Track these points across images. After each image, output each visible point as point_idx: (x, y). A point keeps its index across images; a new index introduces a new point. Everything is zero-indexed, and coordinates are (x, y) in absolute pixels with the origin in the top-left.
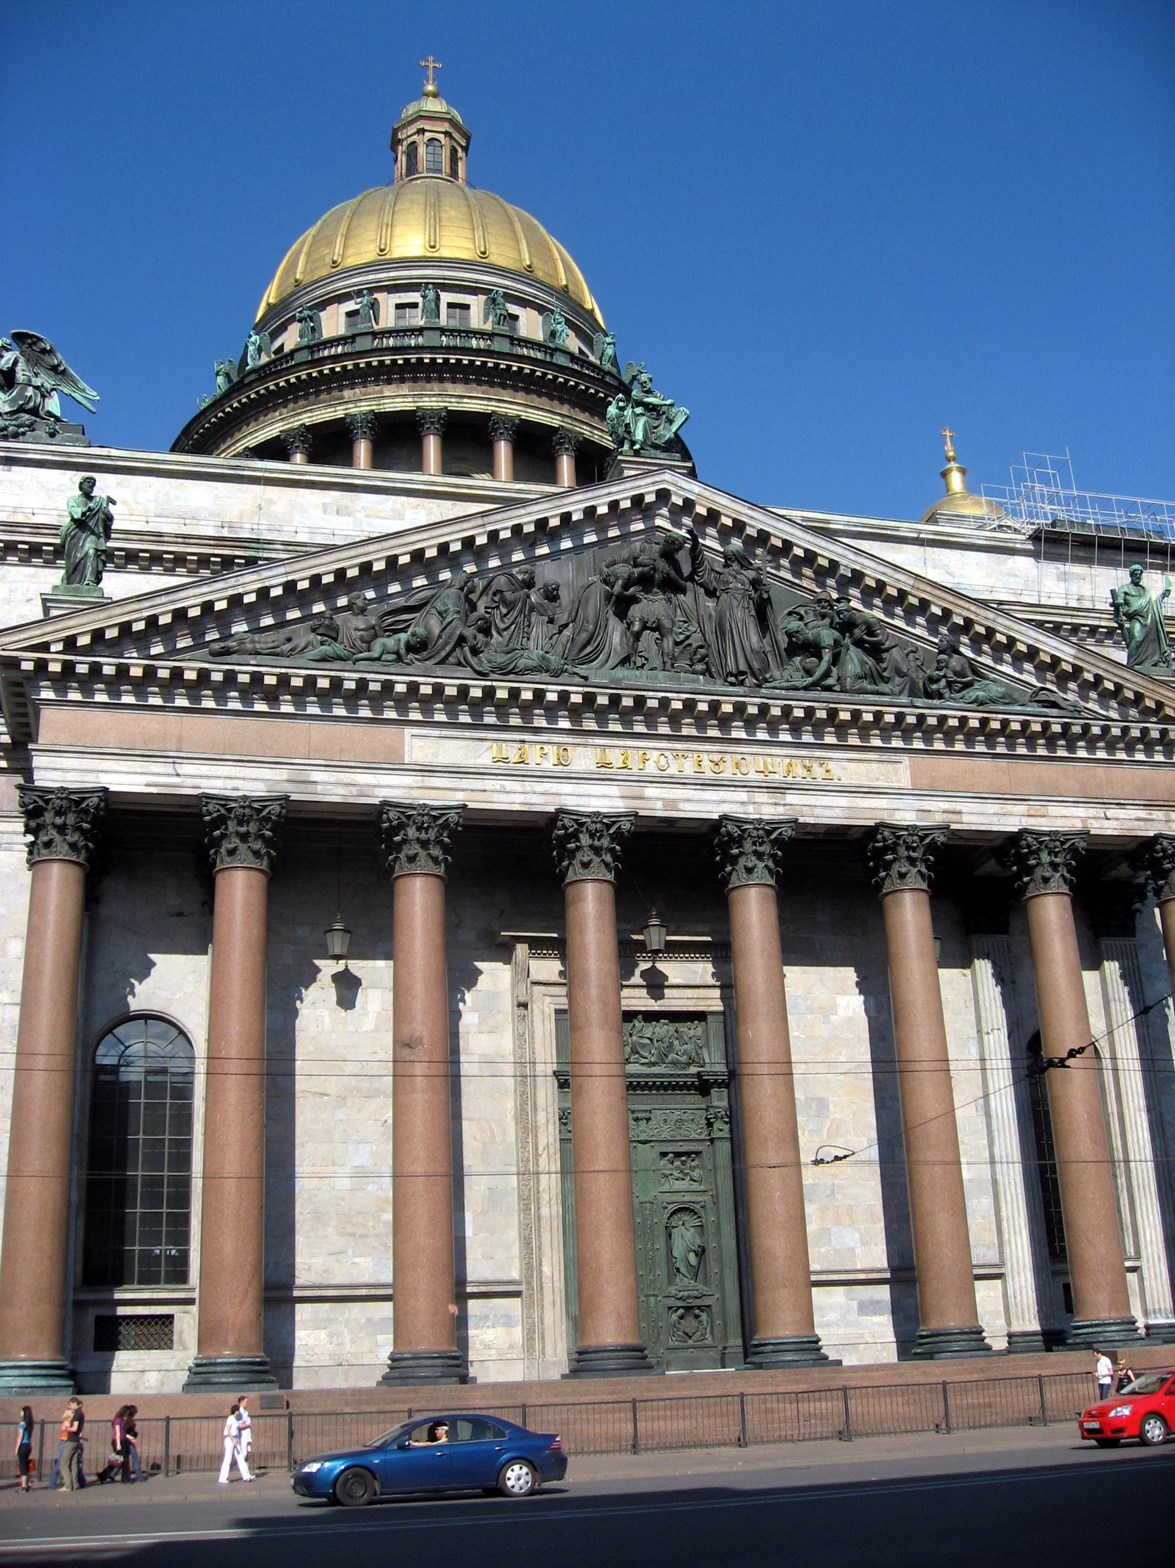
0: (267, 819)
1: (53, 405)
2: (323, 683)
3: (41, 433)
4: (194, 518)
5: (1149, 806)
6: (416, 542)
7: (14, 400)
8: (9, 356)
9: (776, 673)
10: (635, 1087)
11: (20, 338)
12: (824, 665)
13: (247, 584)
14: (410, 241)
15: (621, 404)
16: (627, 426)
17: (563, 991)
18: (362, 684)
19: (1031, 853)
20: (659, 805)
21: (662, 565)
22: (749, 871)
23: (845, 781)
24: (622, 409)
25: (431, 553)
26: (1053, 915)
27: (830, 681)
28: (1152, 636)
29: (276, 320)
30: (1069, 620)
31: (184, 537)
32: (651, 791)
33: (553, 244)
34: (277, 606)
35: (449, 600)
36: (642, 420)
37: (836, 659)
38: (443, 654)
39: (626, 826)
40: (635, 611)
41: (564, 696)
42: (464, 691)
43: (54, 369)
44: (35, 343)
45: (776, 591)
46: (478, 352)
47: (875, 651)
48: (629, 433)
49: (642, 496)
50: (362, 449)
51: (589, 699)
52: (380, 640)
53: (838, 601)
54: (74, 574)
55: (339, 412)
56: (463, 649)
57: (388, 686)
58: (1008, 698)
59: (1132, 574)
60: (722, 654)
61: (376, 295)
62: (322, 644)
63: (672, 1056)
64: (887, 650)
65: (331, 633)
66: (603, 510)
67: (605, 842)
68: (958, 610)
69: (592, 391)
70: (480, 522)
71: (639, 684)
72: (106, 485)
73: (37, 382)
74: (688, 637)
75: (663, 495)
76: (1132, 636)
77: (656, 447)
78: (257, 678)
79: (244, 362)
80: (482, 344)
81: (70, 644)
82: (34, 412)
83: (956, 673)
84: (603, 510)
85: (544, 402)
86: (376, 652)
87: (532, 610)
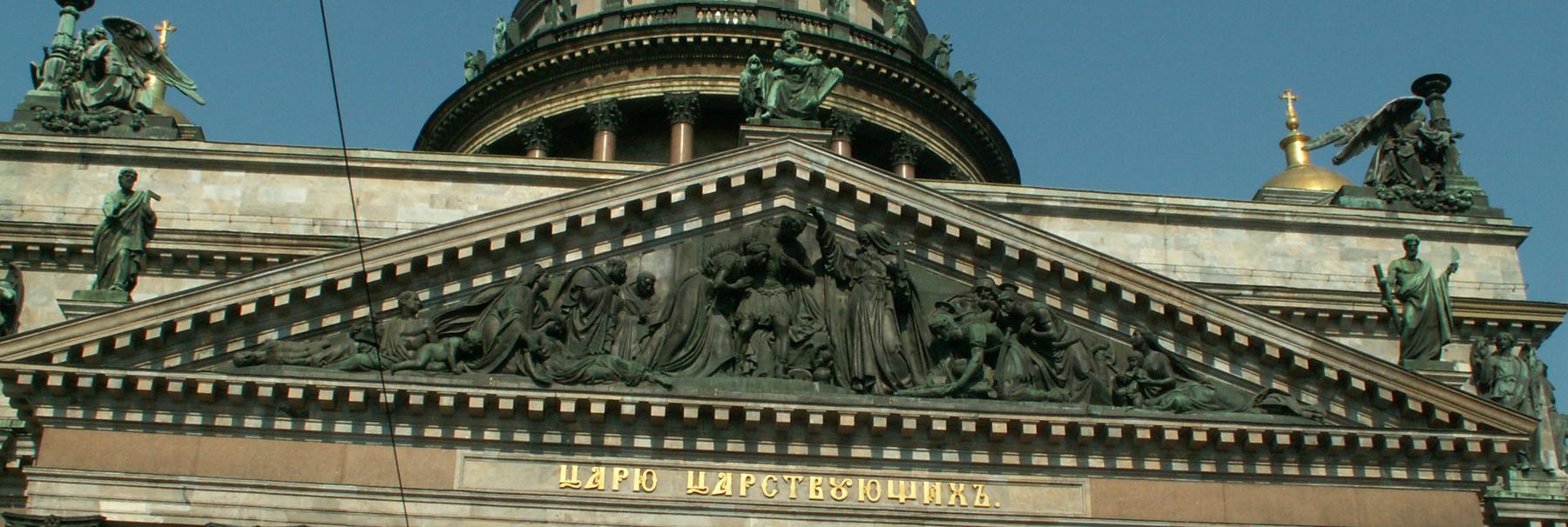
3: (125, 128)
4: (283, 216)
7: (102, 92)
8: (99, 46)
12: (973, 365)
13: (279, 284)
15: (754, 66)
16: (758, 91)
21: (778, 250)
24: (755, 72)
27: (981, 386)
28: (1431, 323)
30: (1350, 308)
31: (264, 236)
34: (314, 309)
35: (515, 300)
37: (991, 359)
38: (499, 361)
41: (643, 409)
44: (128, 30)
45: (923, 280)
47: (1043, 345)
48: (760, 99)
50: (605, 141)
52: (428, 346)
53: (1002, 287)
54: (104, 278)
55: (580, 102)
59: (1407, 245)
62: (360, 350)
64: (1065, 347)
65: (370, 335)
68: (1156, 296)
69: (872, 67)
70: (558, 207)
71: (735, 394)
72: (146, 179)
74: (808, 337)
75: (786, 170)
83: (1152, 374)
84: (710, 189)
87: (619, 309)
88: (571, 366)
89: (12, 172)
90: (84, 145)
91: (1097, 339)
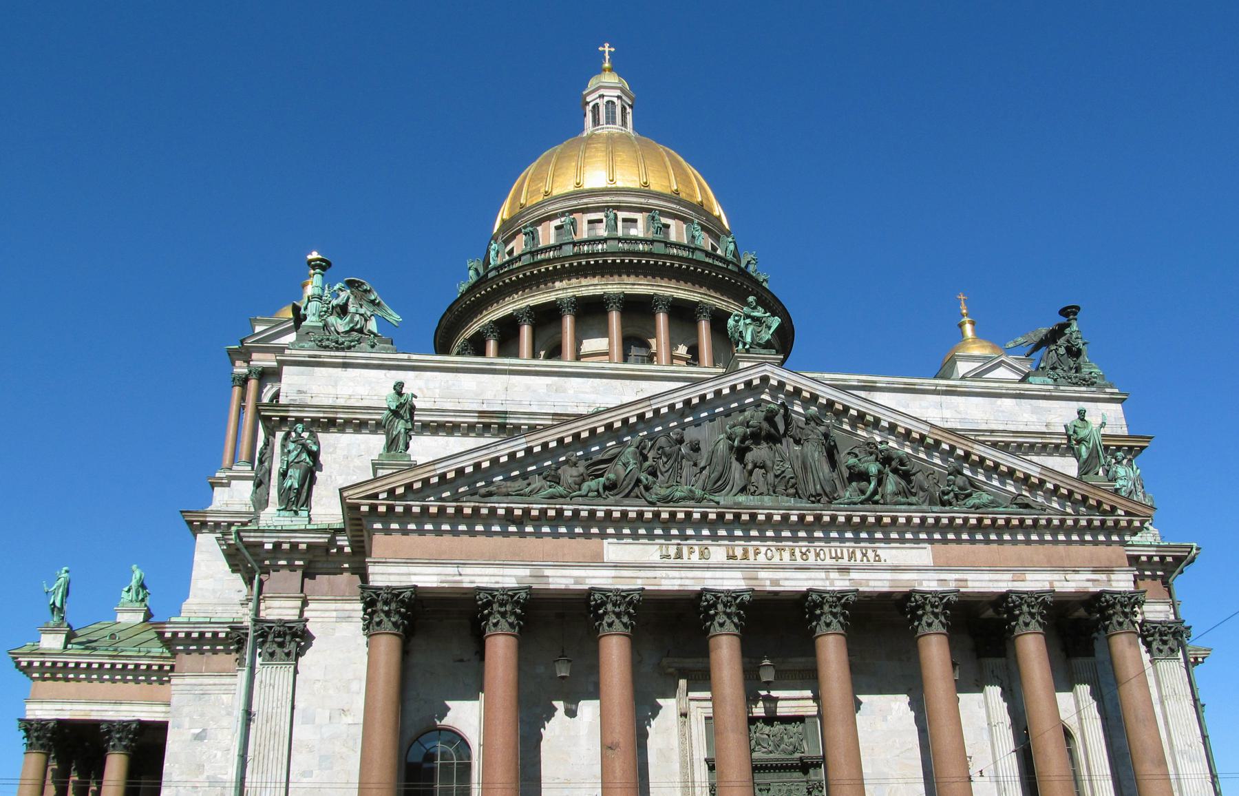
0: (517, 602)
1: (372, 325)
2: (552, 513)
5: (1095, 571)
6: (607, 418)
9: (841, 493)
10: (757, 768)
11: (350, 284)
14: (595, 176)
17: (710, 704)
18: (576, 513)
19: (1015, 607)
20: (768, 583)
21: (765, 425)
22: (828, 625)
23: (889, 562)
24: (737, 321)
25: (618, 425)
26: (1032, 648)
27: (877, 497)
29: (510, 231)
32: (762, 574)
33: (691, 171)
36: (750, 328)
37: (880, 482)
39: (747, 597)
40: (749, 457)
41: (704, 516)
42: (640, 514)
43: (373, 302)
46: (643, 254)
47: (906, 476)
49: (751, 381)
51: (721, 516)
55: (551, 297)
56: (636, 489)
57: (592, 513)
58: (994, 504)
60: (806, 482)
61: (575, 215)
63: (783, 746)
66: (726, 391)
67: (733, 609)
73: (362, 311)
75: (765, 379)
76: (1080, 456)
77: (759, 345)
78: (509, 511)
79: (486, 262)
80: (647, 248)
81: (391, 492)
82: (361, 331)
84: (726, 391)
85: (689, 286)
86: (583, 492)
87: (683, 458)
88: (664, 492)
89: (303, 374)
90: (345, 357)
91: (928, 469)
